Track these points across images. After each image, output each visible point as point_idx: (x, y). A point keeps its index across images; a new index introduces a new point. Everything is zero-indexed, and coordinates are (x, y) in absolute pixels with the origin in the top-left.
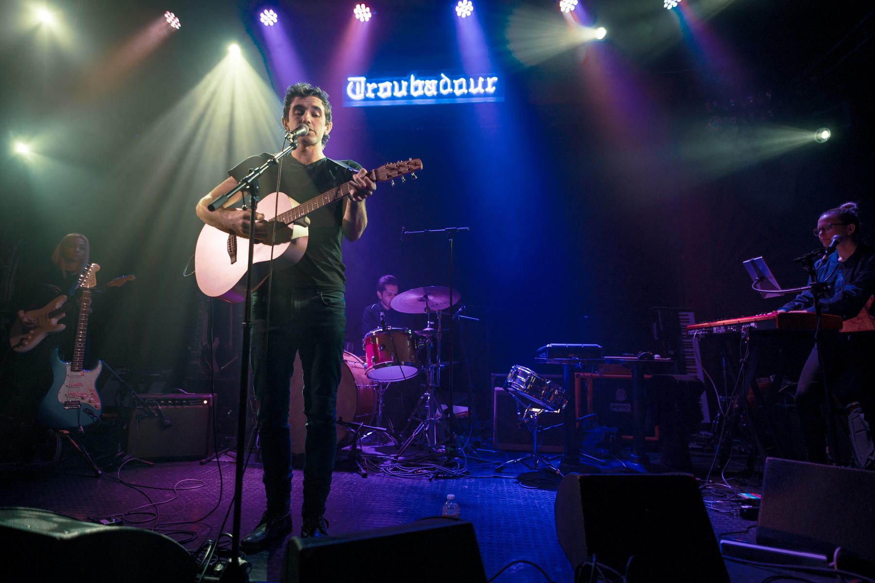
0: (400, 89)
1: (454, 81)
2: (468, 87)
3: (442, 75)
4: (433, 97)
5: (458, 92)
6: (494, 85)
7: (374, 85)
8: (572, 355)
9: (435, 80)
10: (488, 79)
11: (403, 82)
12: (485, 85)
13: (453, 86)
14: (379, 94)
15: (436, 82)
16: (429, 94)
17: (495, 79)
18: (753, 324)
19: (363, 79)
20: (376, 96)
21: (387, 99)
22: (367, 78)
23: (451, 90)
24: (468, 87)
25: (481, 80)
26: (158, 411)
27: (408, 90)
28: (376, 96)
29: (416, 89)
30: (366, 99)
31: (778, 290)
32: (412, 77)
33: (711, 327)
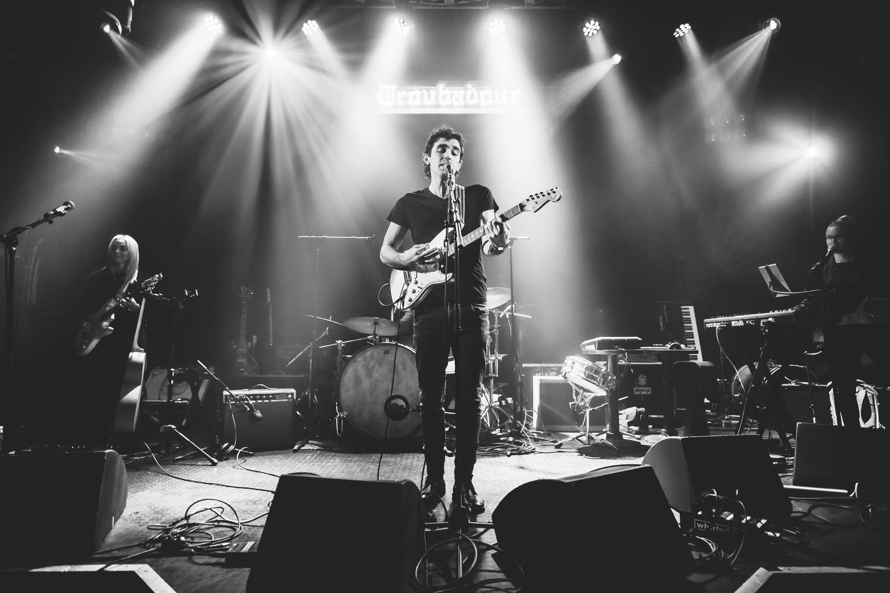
0: (429, 97)
1: (481, 92)
7: (404, 93)
8: (617, 347)
13: (479, 97)
15: (464, 92)
18: (770, 319)
26: (248, 404)
29: (444, 98)
31: (789, 292)
33: (731, 321)
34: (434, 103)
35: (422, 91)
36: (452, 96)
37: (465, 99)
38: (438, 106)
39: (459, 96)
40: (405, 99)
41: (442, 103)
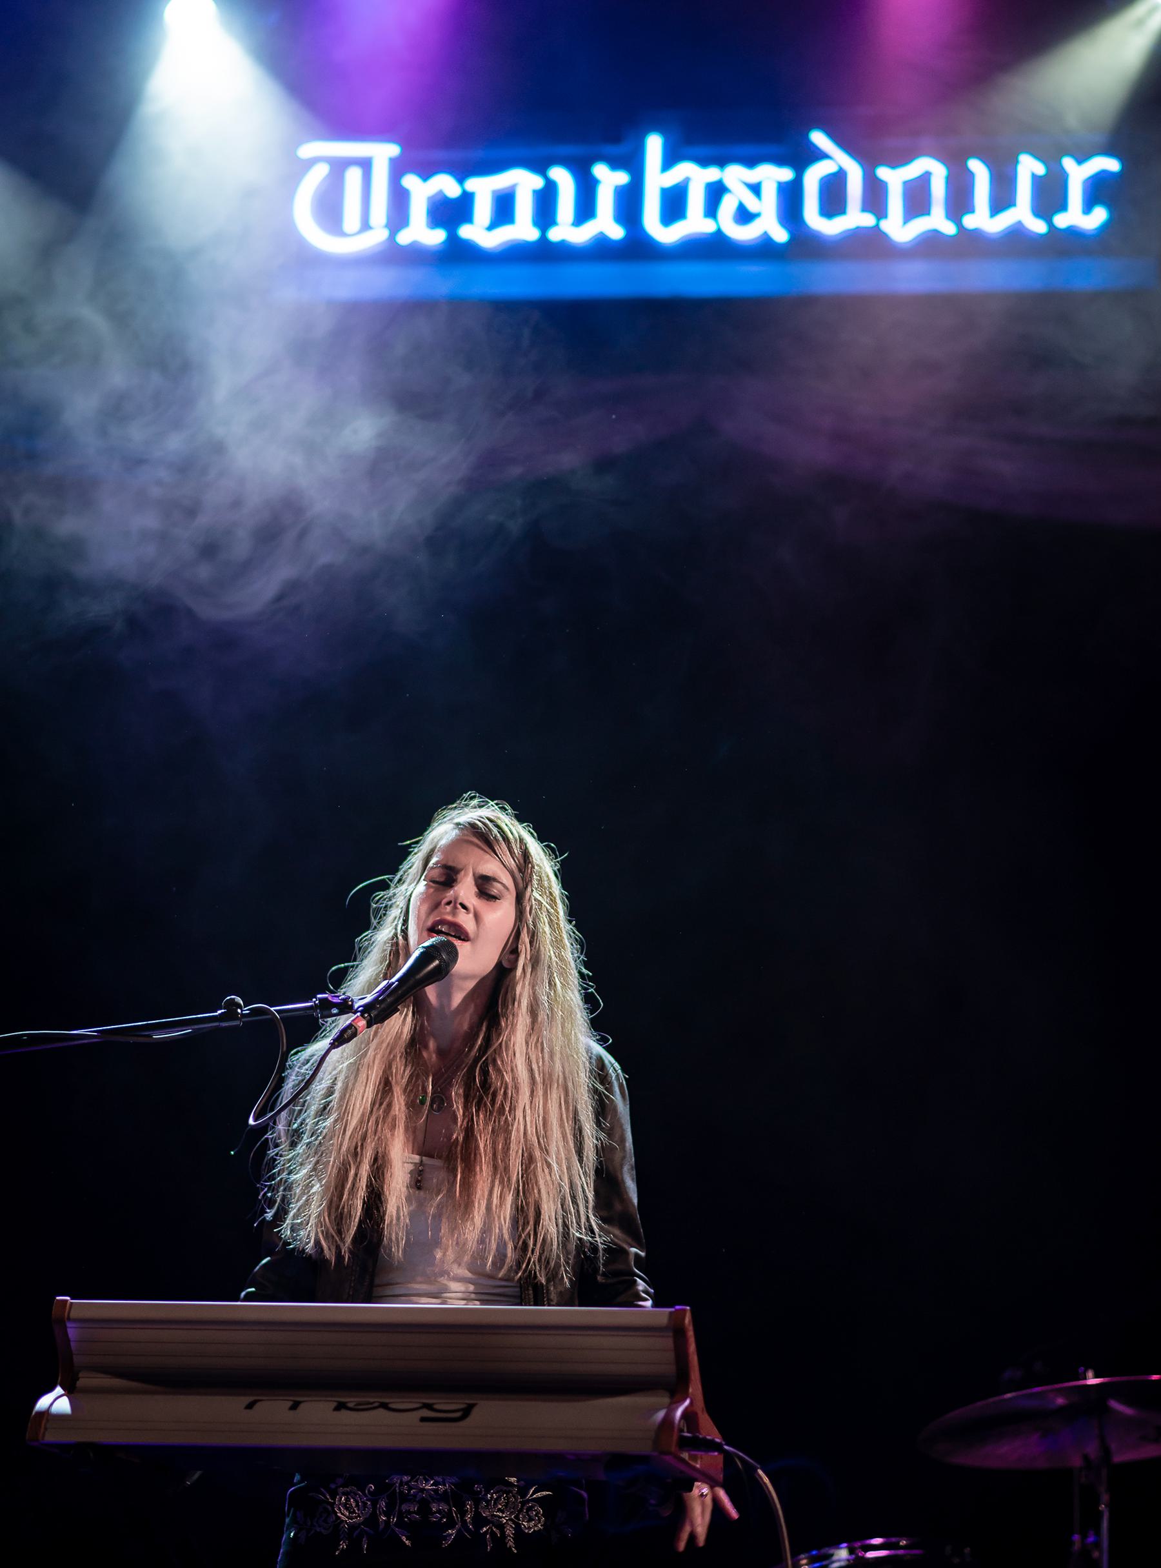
0: (585, 209)
1: (883, 172)
2: (959, 202)
3: (819, 138)
4: (764, 249)
7: (446, 185)
9: (780, 161)
10: (1068, 163)
11: (600, 170)
13: (875, 197)
14: (466, 232)
15: (786, 174)
16: (742, 234)
19: (384, 153)
20: (453, 239)
21: (517, 254)
22: (406, 143)
23: (867, 220)
24: (959, 202)
25: (1029, 167)
28: (453, 239)
32: (654, 145)
34: (617, 232)
36: (716, 192)
39: (756, 189)
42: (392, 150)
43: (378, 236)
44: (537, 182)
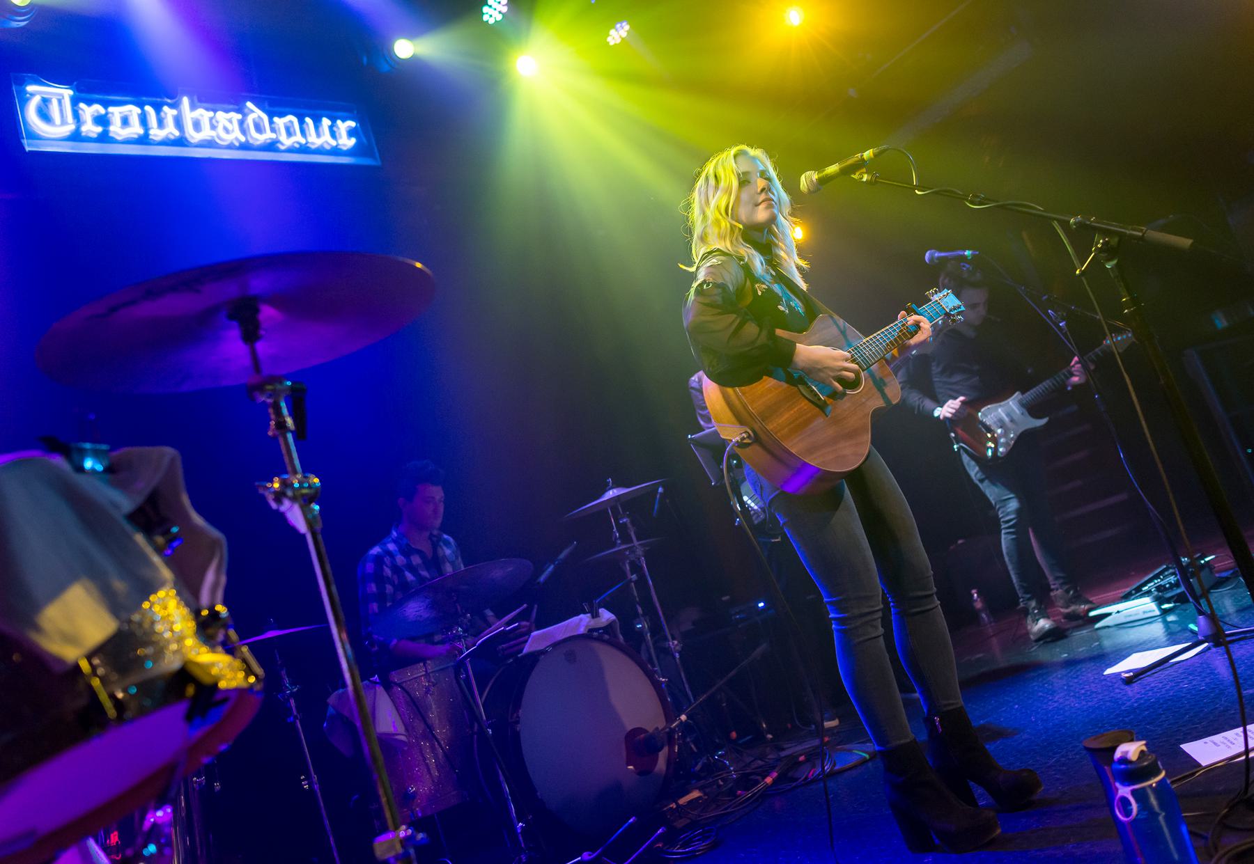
0: (161, 123)
1: (276, 119)
3: (249, 104)
5: (287, 142)
6: (351, 133)
7: (98, 109)
10: (339, 122)
11: (165, 108)
12: (333, 135)
13: (273, 130)
15: (239, 116)
17: (352, 124)
19: (67, 93)
22: (78, 89)
23: (273, 136)
25: (326, 122)
27: (178, 122)
29: (197, 126)
30: (76, 136)
32: (185, 101)
35: (142, 107)
37: (244, 131)
38: (181, 142)
39: (230, 121)
40: (102, 121)
41: (194, 136)
42: (71, 92)
43: (71, 127)
44: (138, 110)
